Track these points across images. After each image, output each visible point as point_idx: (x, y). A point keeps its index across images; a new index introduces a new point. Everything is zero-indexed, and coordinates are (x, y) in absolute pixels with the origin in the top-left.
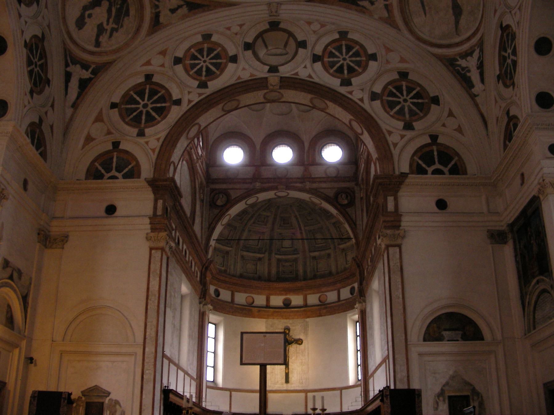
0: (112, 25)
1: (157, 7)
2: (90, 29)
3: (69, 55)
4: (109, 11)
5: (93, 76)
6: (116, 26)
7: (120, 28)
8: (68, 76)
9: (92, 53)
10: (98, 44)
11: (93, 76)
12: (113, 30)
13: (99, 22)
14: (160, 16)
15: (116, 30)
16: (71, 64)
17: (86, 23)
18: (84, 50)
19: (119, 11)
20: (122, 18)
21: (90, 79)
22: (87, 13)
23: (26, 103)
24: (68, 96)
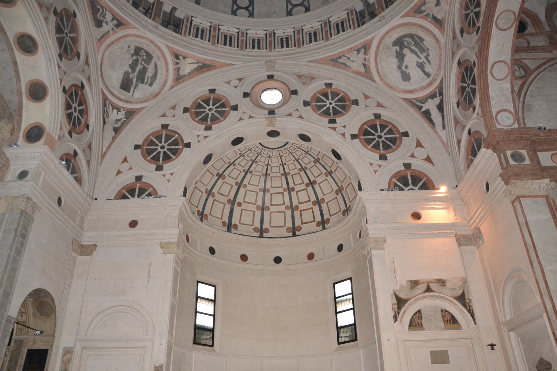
0: (423, 56)
1: (428, 15)
2: (415, 73)
3: (417, 101)
4: (412, 51)
5: (441, 97)
6: (425, 54)
7: (428, 51)
8: (427, 115)
9: (430, 84)
10: (428, 75)
11: (441, 97)
12: (427, 57)
13: (415, 64)
14: (436, 17)
15: (428, 55)
16: (422, 105)
17: (409, 73)
18: (424, 88)
19: (416, 44)
20: (422, 45)
21: (442, 101)
22: (403, 68)
23: (377, 168)
24: (435, 126)
